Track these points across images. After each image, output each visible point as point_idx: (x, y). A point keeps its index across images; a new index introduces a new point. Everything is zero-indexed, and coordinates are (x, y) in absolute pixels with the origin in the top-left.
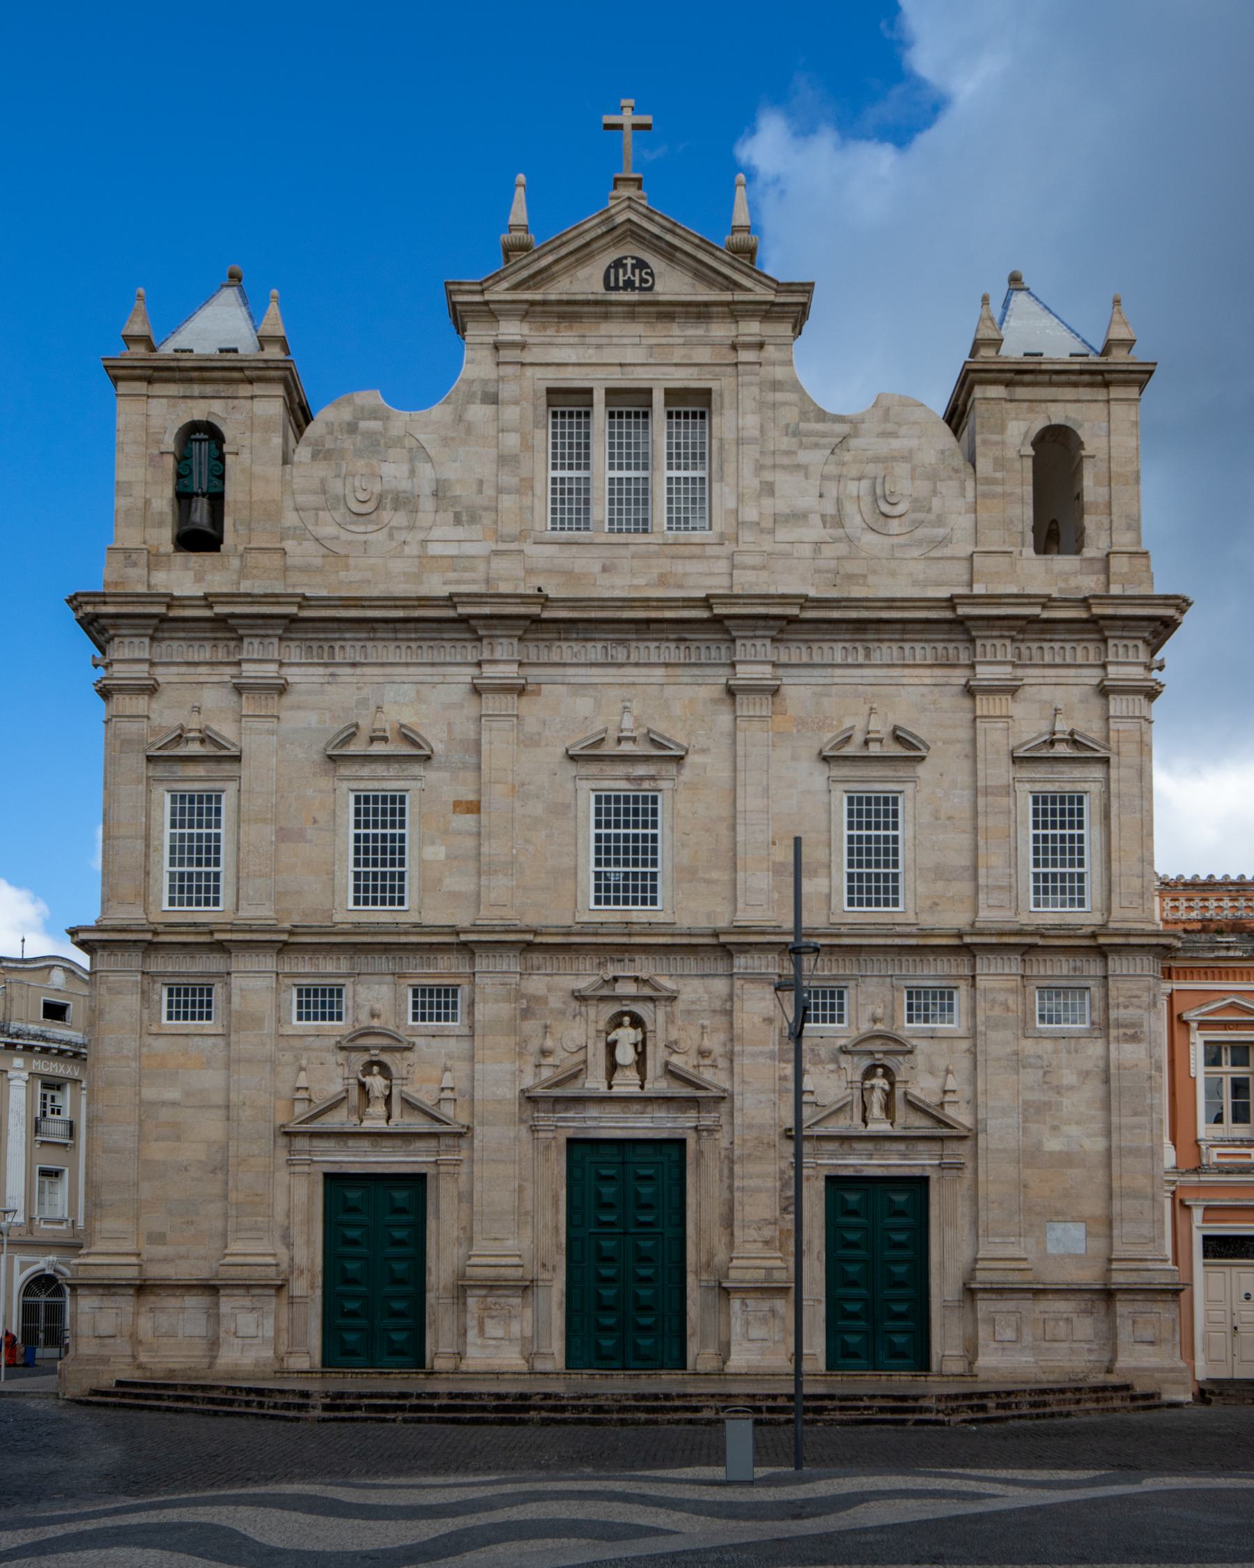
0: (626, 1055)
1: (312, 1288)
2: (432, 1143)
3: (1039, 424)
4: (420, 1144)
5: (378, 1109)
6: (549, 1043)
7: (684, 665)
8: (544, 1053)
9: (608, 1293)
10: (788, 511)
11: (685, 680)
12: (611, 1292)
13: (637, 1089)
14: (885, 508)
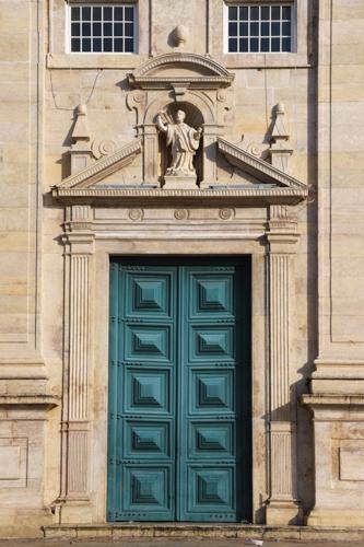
1: (95, 410)
2: (260, 213)
4: (244, 214)
5: (185, 164)
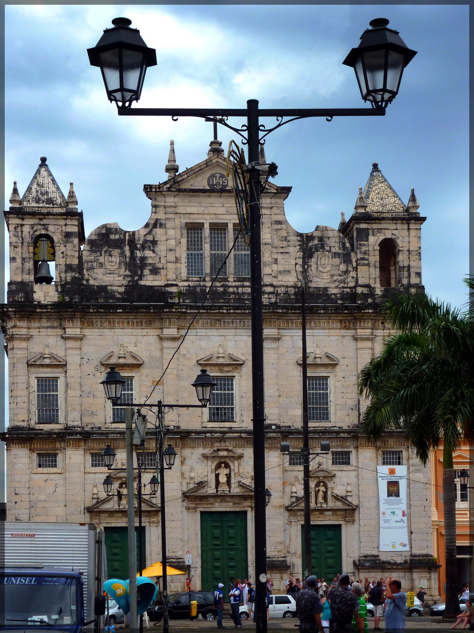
0: (223, 479)
3: (382, 238)
6: (192, 475)
7: (243, 329)
8: (191, 478)
9: (217, 572)
10: (282, 270)
11: (242, 334)
12: (219, 572)
13: (228, 492)
14: (321, 269)
